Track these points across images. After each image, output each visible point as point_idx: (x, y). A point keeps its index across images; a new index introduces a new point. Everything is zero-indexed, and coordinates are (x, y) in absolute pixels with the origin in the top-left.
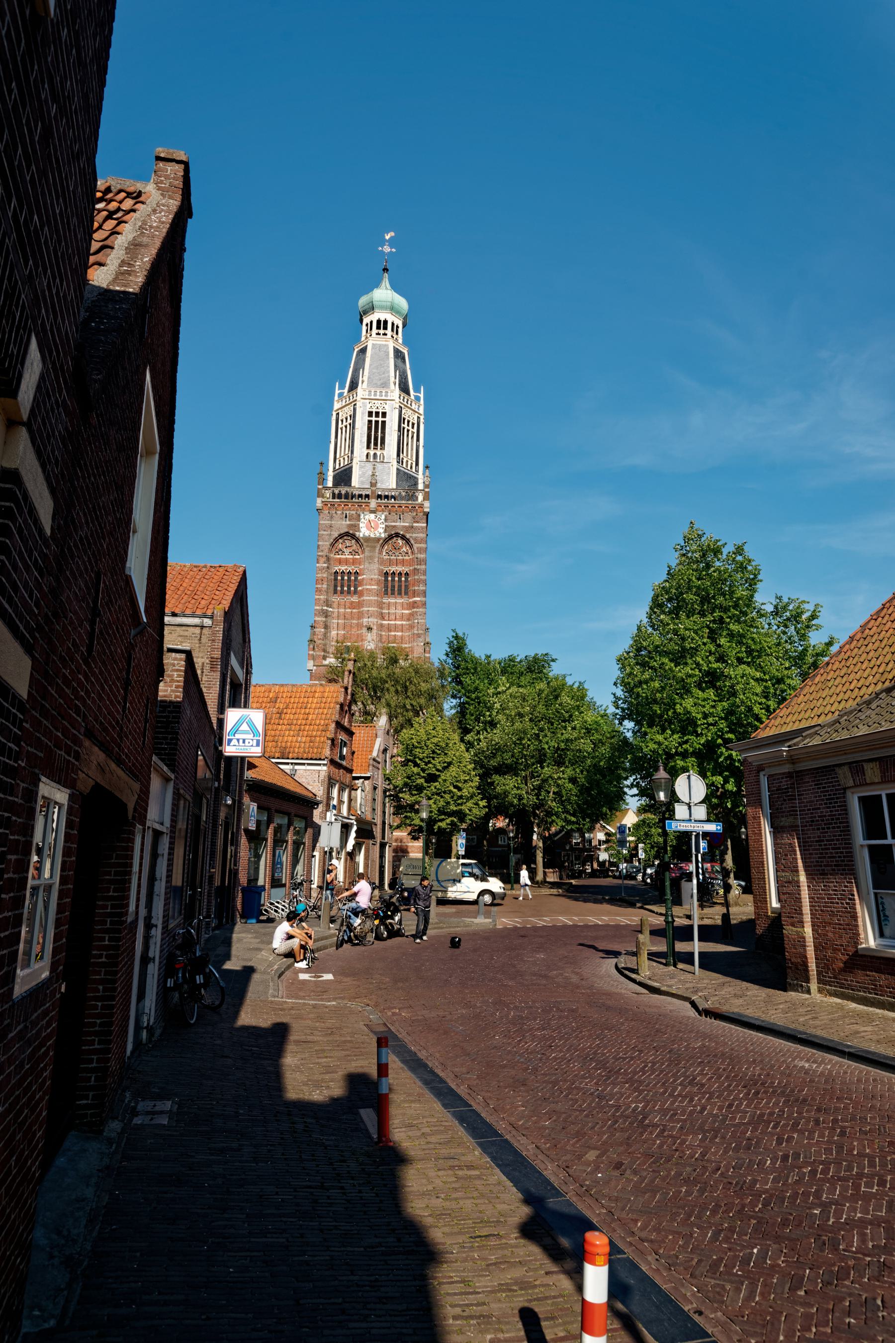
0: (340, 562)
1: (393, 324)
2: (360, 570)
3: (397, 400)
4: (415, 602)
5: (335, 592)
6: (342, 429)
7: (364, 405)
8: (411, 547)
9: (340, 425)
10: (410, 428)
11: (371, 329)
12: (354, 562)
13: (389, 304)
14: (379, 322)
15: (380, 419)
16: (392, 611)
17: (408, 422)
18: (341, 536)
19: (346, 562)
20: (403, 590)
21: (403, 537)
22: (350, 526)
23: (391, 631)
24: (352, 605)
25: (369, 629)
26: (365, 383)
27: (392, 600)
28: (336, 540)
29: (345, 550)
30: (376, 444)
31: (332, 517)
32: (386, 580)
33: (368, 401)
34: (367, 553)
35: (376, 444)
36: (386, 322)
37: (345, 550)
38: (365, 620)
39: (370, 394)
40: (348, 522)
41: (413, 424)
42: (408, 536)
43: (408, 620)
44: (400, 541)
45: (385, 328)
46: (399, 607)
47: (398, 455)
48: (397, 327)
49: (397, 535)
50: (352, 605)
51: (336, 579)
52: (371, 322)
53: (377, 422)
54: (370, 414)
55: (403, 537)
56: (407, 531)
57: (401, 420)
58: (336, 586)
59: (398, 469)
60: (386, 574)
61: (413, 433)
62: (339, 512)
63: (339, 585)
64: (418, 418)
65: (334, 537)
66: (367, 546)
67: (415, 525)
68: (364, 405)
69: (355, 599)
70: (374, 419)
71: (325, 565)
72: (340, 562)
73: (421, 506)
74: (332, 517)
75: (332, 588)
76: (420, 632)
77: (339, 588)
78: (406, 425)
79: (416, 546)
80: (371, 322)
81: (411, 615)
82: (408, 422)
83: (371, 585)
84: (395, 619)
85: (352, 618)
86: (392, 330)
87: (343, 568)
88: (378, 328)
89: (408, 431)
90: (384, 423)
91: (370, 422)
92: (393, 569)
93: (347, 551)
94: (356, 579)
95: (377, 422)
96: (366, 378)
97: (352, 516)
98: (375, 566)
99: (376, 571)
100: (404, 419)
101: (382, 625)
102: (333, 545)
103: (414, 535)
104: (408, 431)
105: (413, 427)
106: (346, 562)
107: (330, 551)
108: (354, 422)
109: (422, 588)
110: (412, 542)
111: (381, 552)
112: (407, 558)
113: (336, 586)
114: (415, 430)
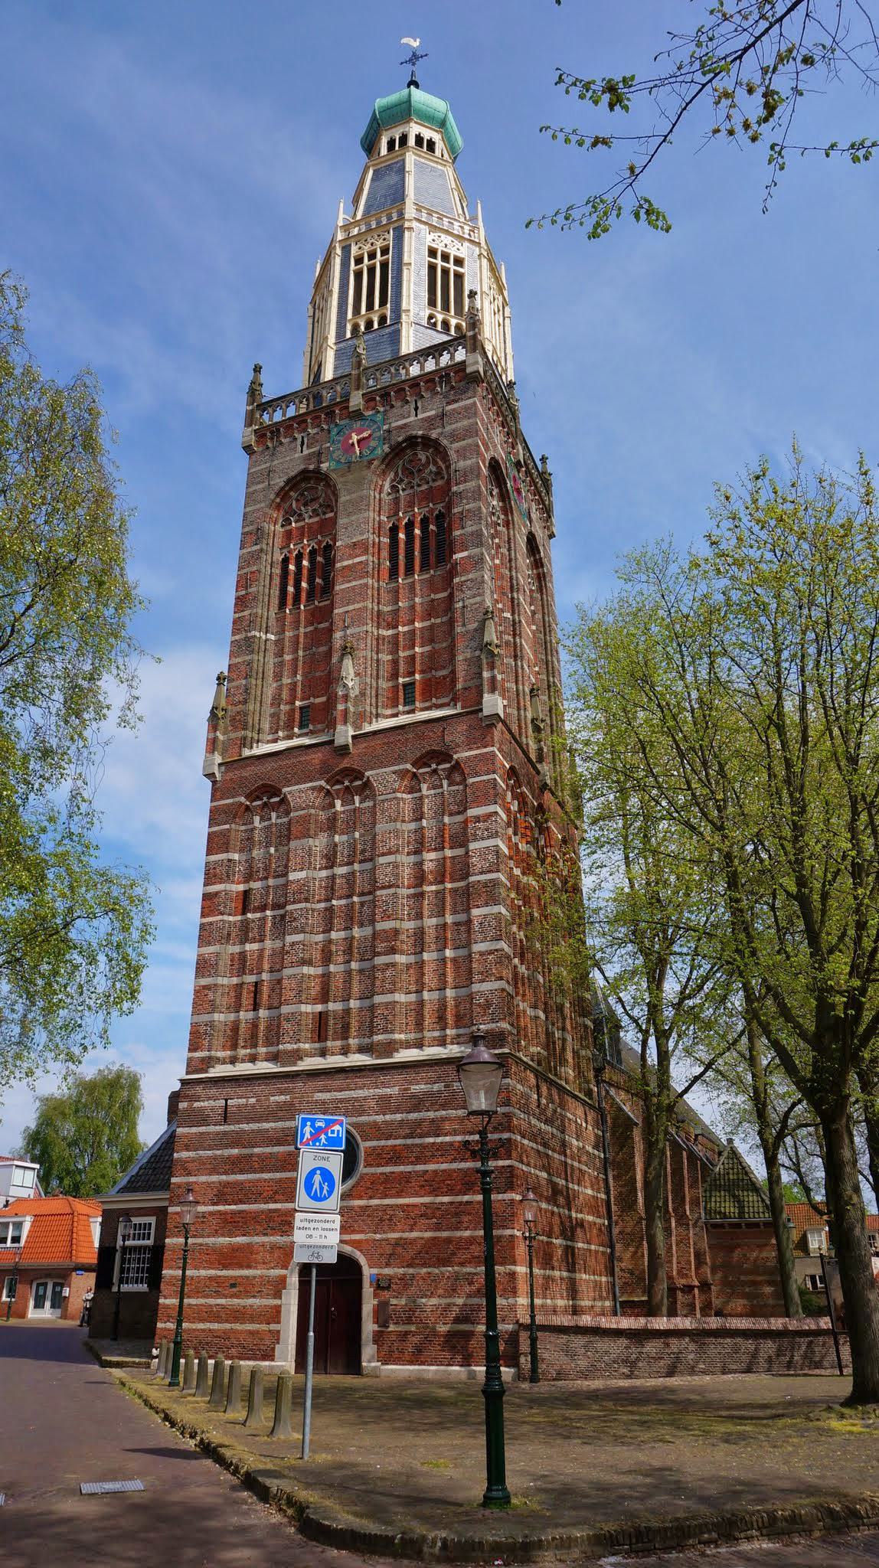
1: (419, 140)
7: (346, 249)
14: (391, 144)
18: (293, 483)
21: (428, 442)
22: (309, 457)
34: (343, 498)
36: (404, 139)
40: (306, 452)
42: (434, 435)
44: (422, 456)
49: (412, 441)
54: (359, 260)
65: (277, 488)
68: (346, 249)
71: (258, 547)
77: (291, 589)
83: (351, 557)
91: (358, 275)
95: (371, 270)
103: (448, 428)
109: (469, 529)
110: (445, 442)
112: (440, 483)
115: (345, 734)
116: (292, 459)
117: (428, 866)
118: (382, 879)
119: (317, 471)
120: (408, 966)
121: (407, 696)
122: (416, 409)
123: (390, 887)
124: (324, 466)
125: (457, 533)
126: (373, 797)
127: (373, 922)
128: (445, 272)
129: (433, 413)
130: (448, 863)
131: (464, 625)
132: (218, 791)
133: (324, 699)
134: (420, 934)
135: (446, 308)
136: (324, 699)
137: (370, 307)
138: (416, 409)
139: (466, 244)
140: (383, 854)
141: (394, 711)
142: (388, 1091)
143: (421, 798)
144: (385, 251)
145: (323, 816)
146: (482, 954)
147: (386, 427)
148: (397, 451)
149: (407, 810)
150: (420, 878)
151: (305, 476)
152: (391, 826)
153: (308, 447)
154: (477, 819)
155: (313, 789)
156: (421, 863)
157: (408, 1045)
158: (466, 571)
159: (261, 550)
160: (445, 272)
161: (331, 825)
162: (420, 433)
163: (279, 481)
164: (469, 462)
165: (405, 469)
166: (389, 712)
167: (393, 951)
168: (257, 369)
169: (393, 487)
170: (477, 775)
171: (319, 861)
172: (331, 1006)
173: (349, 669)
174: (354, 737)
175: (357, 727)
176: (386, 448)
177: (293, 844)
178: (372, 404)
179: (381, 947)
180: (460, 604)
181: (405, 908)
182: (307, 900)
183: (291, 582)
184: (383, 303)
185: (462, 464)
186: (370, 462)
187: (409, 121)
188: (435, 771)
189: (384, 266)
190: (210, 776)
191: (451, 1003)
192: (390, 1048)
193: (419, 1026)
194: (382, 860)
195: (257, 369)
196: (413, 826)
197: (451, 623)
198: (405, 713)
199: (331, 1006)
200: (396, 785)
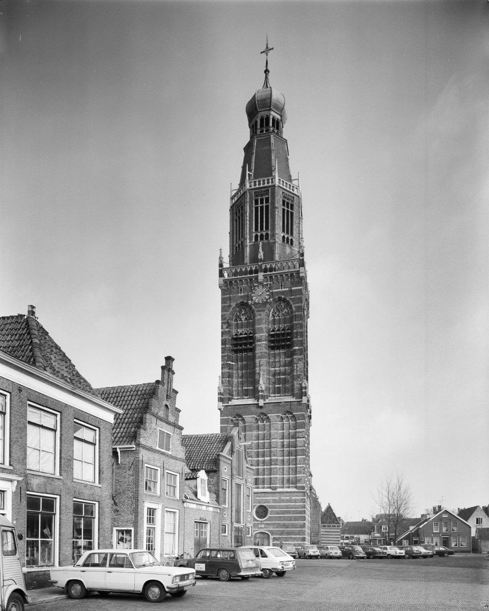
1: (273, 120)
6: (236, 220)
8: (291, 308)
11: (256, 129)
14: (262, 120)
21: (284, 300)
36: (268, 118)
40: (242, 294)
49: (280, 299)
67: (293, 288)
71: (227, 330)
76: (298, 373)
90: (267, 207)
91: (257, 209)
95: (262, 208)
110: (291, 303)
115: (261, 402)
117: (285, 443)
118: (273, 445)
119: (247, 304)
120: (280, 468)
121: (278, 391)
122: (282, 286)
123: (275, 448)
124: (250, 302)
125: (294, 339)
126: (270, 422)
127: (270, 456)
128: (288, 211)
129: (287, 289)
130: (291, 443)
131: (297, 372)
132: (222, 413)
133: (252, 388)
134: (283, 461)
135: (288, 233)
136: (252, 388)
137: (262, 229)
138: (282, 286)
140: (273, 439)
141: (274, 395)
142: (275, 498)
143: (283, 424)
145: (255, 425)
146: (300, 467)
147: (271, 291)
149: (279, 426)
150: (283, 446)
151: (242, 304)
152: (276, 431)
153: (243, 293)
154: (299, 432)
155: (253, 417)
156: (283, 442)
157: (280, 487)
159: (229, 331)
160: (288, 211)
161: (258, 428)
162: (283, 297)
164: (299, 313)
165: (277, 308)
166: (272, 395)
167: (276, 464)
169: (273, 315)
170: (300, 420)
171: (254, 438)
172: (259, 477)
173: (261, 382)
174: (264, 404)
175: (265, 400)
176: (271, 299)
177: (247, 433)
178: (266, 279)
179: (273, 463)
180: (296, 365)
181: (279, 453)
182: (252, 449)
184: (267, 228)
187: (270, 110)
188: (287, 417)
189: (267, 207)
190: (220, 409)
191: (291, 478)
192: (275, 488)
193: (283, 483)
194: (273, 440)
196: (282, 431)
197: (292, 371)
198: (278, 396)
199: (259, 477)
200: (277, 420)
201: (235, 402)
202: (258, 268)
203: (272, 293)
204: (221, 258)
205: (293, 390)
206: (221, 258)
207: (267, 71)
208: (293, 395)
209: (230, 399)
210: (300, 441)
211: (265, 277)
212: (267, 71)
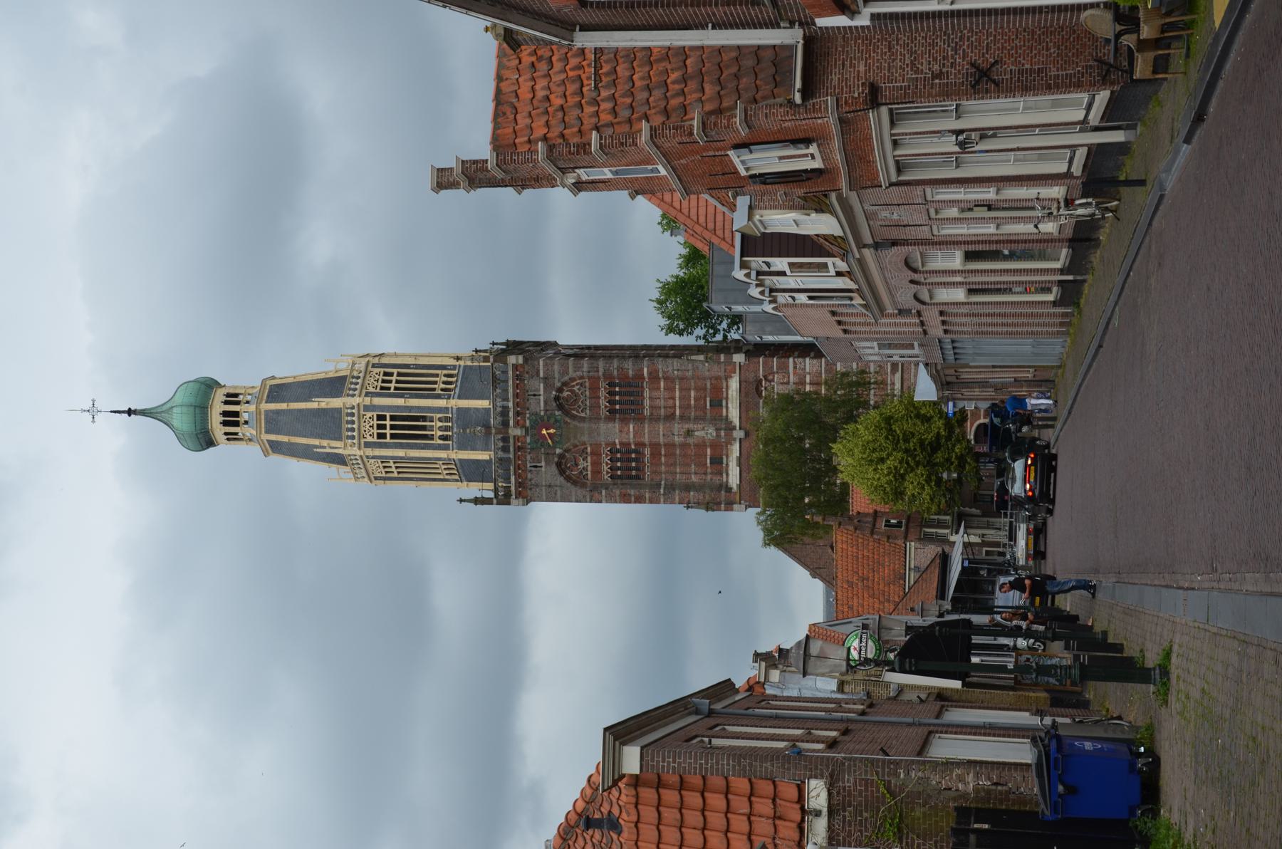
0: (596, 472)
1: (226, 403)
2: (607, 445)
3: (356, 401)
4: (650, 373)
5: (637, 477)
8: (573, 379)
9: (396, 475)
10: (394, 378)
12: (596, 454)
13: (198, 411)
14: (225, 423)
15: (388, 423)
16: (662, 403)
17: (384, 381)
18: (562, 472)
19: (597, 464)
20: (632, 389)
22: (547, 463)
23: (689, 405)
24: (656, 454)
25: (689, 433)
26: (334, 443)
27: (647, 403)
28: (568, 479)
29: (581, 467)
30: (424, 428)
31: (537, 486)
32: (619, 411)
33: (363, 441)
34: (585, 438)
35: (424, 428)
36: (225, 414)
37: (581, 467)
38: (676, 439)
39: (353, 437)
40: (543, 464)
41: (386, 374)
43: (673, 381)
44: (566, 394)
45: (236, 414)
46: (655, 394)
47: (438, 397)
48: (228, 395)
50: (656, 454)
51: (620, 477)
52: (226, 434)
53: (392, 427)
54: (381, 436)
55: (560, 390)
56: (552, 386)
57: (384, 391)
58: (632, 477)
59: (459, 398)
60: (612, 411)
61: (399, 374)
62: (529, 476)
63: (628, 473)
64: (374, 366)
66: (575, 437)
67: (541, 375)
68: (368, 445)
69: (647, 451)
70: (388, 431)
72: (596, 472)
73: (515, 367)
74: (537, 486)
75: (634, 482)
77: (634, 473)
78: (392, 385)
79: (571, 373)
80: (226, 434)
81: (666, 379)
82: (384, 381)
84: (674, 399)
85: (674, 454)
86: (238, 403)
87: (605, 468)
88: (236, 424)
89: (397, 382)
90: (393, 418)
91: (393, 436)
92: (603, 402)
93: (582, 464)
94: (618, 451)
95: (392, 427)
96: (325, 443)
97: (533, 460)
98: (603, 426)
99: (610, 425)
100: (382, 388)
101: (682, 417)
102: (575, 483)
103: (556, 375)
104: (397, 382)
105: (391, 374)
106: (597, 464)
107: (583, 486)
108: (392, 458)
110: (566, 378)
111: (583, 419)
113: (632, 477)
114: (395, 371)
116: (548, 473)
124: (558, 451)
135: (435, 383)
139: (370, 368)
144: (381, 418)
148: (560, 407)
151: (559, 465)
158: (657, 371)
163: (560, 480)
168: (461, 501)
183: (628, 473)
185: (585, 369)
186: (566, 423)
189: (393, 418)
195: (461, 501)
201: (734, 478)
202: (499, 436)
203: (546, 410)
204: (477, 501)
205: (718, 378)
206: (477, 501)
207: (130, 412)
208: (728, 378)
209: (729, 490)
210: (812, 365)
211: (517, 424)
212: (130, 412)
